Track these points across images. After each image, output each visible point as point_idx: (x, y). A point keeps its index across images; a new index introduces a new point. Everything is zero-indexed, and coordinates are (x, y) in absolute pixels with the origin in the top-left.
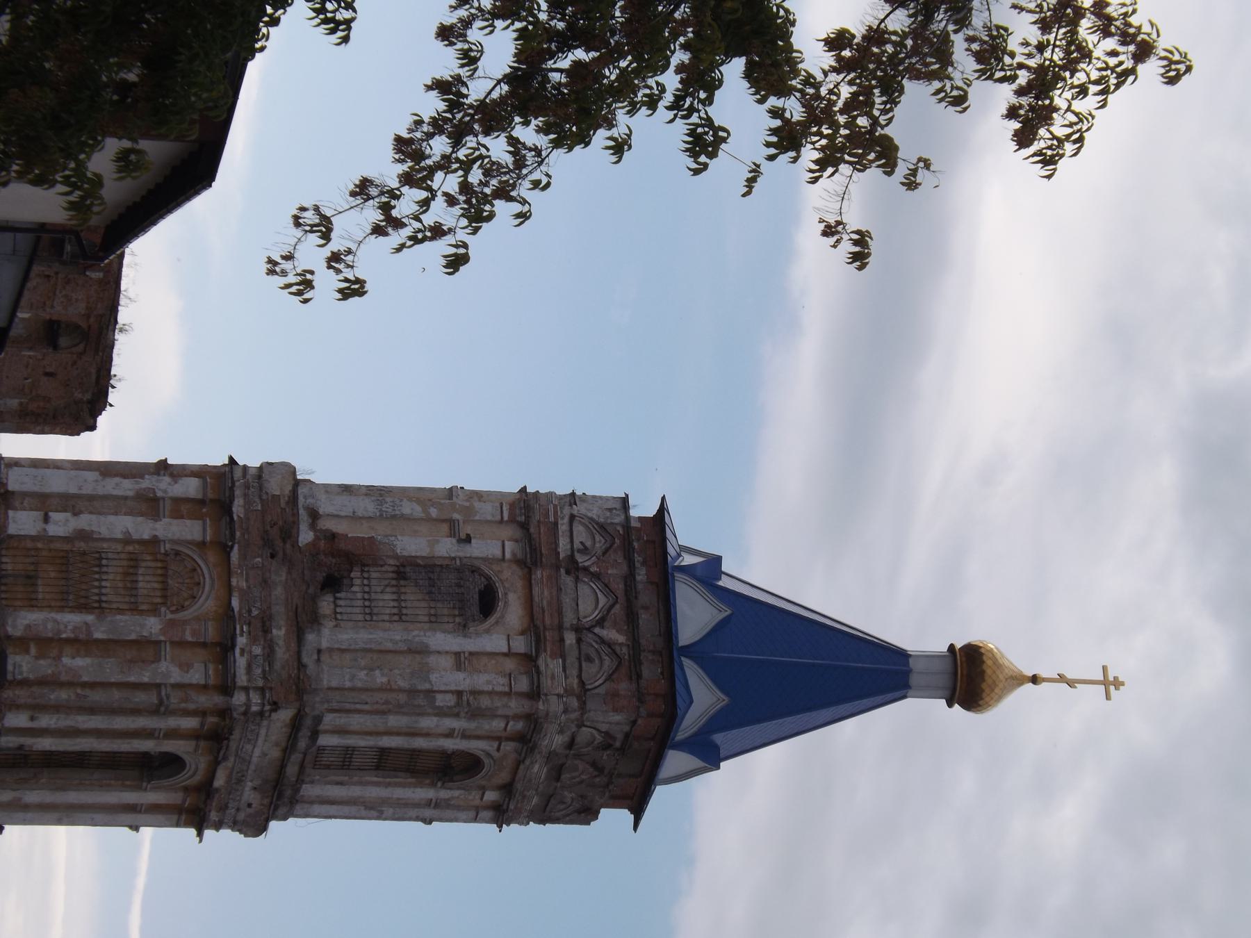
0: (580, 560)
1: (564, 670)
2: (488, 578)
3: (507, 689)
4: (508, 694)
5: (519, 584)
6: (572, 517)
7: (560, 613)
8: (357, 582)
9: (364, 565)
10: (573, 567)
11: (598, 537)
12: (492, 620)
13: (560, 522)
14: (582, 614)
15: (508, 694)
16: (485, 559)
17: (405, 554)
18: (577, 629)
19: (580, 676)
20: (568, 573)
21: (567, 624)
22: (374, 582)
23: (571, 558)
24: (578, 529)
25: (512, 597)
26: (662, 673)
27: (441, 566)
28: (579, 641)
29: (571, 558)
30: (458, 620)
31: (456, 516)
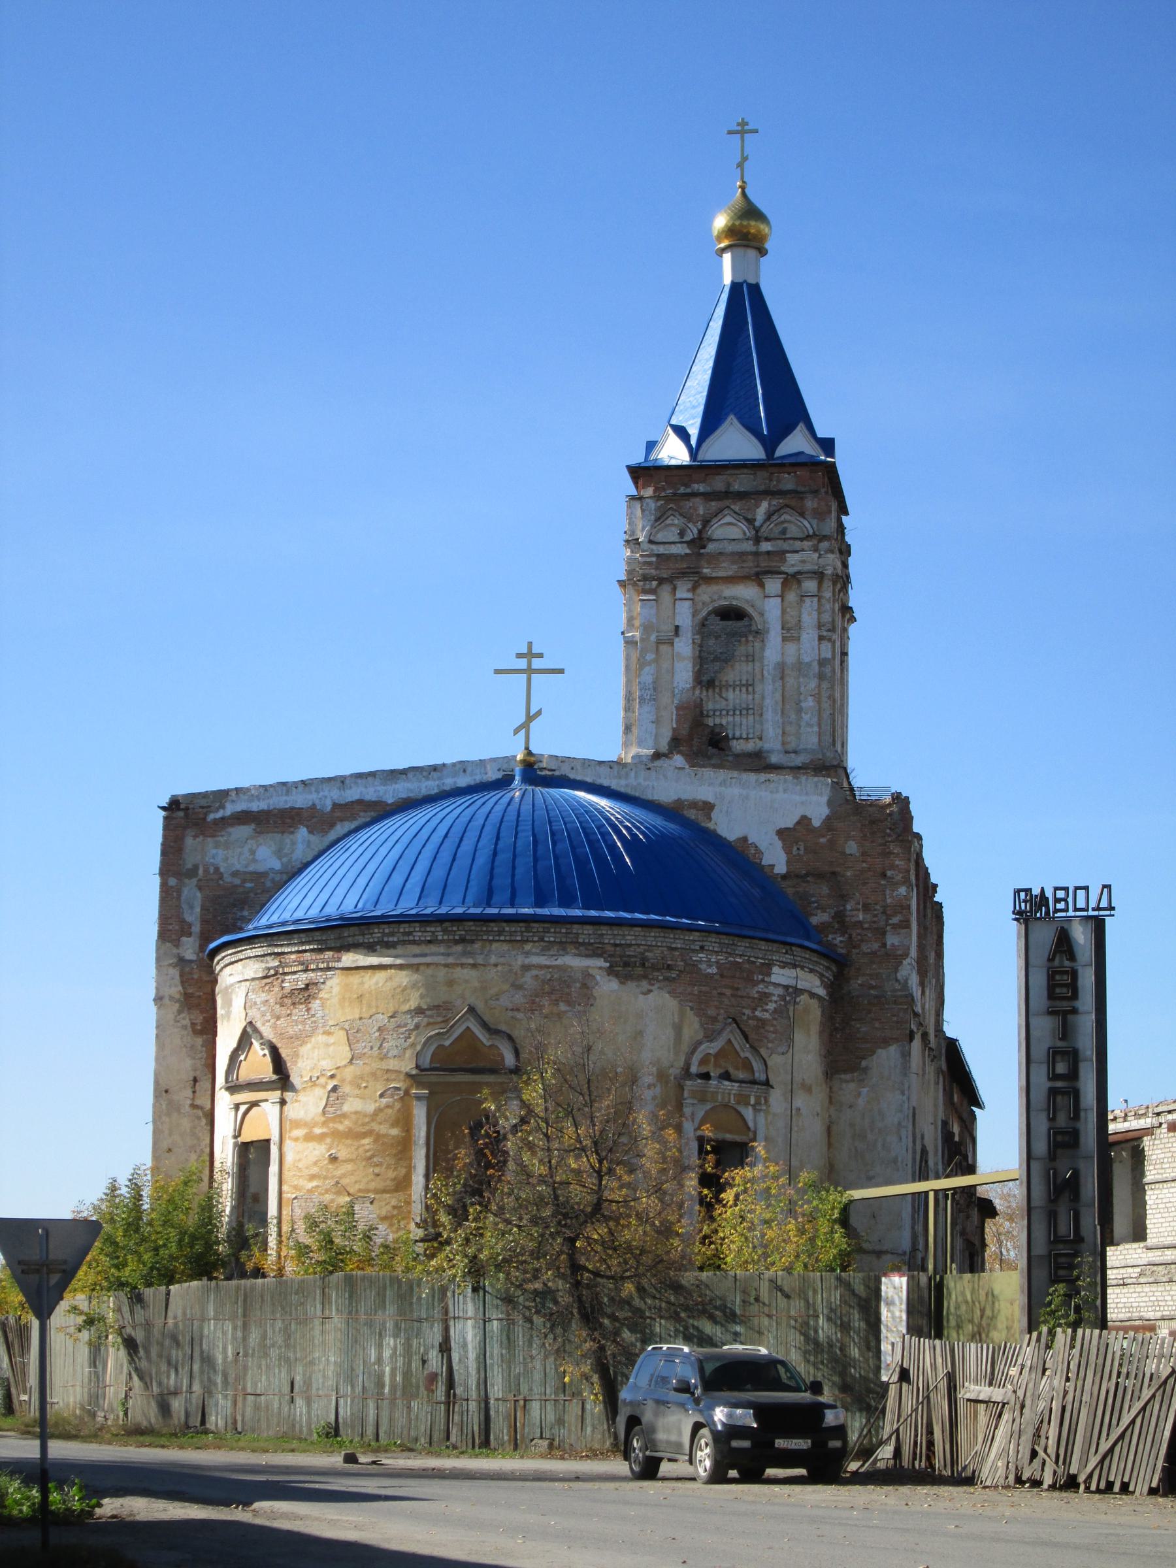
0: (691, 537)
1: (797, 552)
2: (709, 614)
3: (816, 599)
4: (820, 598)
5: (714, 588)
6: (651, 542)
8: (718, 721)
9: (702, 713)
10: (699, 542)
11: (669, 521)
12: (750, 610)
13: (656, 552)
14: (741, 536)
15: (820, 598)
17: (691, 680)
18: (757, 540)
19: (802, 540)
20: (704, 547)
21: (754, 549)
22: (718, 707)
23: (690, 543)
24: (660, 537)
26: (789, 473)
27: (700, 651)
28: (767, 539)
29: (690, 543)
30: (751, 638)
31: (653, 638)
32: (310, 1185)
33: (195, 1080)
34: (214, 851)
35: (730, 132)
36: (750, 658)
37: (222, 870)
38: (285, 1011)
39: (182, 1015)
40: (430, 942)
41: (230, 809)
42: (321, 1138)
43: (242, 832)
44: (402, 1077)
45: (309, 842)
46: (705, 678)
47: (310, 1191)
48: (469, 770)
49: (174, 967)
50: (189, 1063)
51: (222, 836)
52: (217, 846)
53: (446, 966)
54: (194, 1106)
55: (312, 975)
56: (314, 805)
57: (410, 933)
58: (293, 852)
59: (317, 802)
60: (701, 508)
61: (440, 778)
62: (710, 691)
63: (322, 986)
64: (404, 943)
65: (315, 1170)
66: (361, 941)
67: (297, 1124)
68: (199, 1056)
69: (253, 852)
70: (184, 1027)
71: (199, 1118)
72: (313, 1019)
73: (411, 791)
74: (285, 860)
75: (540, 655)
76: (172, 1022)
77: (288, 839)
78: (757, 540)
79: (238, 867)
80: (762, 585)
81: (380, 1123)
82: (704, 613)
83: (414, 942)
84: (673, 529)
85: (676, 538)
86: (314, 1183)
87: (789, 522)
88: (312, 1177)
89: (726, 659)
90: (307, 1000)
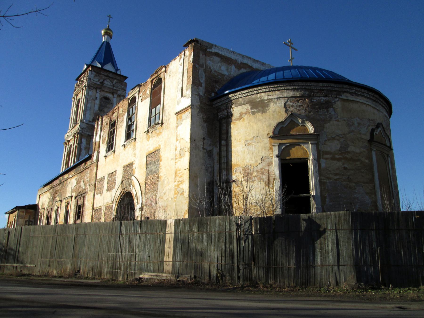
2: (102, 97)
10: (102, 83)
14: (110, 85)
16: (100, 96)
19: (121, 89)
20: (103, 84)
23: (101, 83)
24: (94, 80)
25: (106, 94)
28: (115, 87)
29: (101, 83)
31: (91, 98)
33: (204, 138)
34: (209, 62)
35: (107, 16)
37: (212, 69)
39: (199, 114)
40: (368, 98)
41: (213, 50)
42: (339, 160)
43: (217, 59)
45: (235, 70)
47: (336, 180)
49: (198, 96)
51: (211, 58)
52: (210, 60)
54: (203, 148)
56: (236, 60)
57: (363, 93)
59: (237, 60)
60: (104, 77)
62: (101, 112)
63: (334, 104)
64: (362, 95)
65: (338, 172)
66: (349, 91)
69: (220, 67)
70: (200, 118)
74: (229, 73)
78: (113, 86)
79: (216, 70)
80: (113, 95)
82: (102, 97)
83: (364, 96)
84: (97, 79)
85: (98, 81)
86: (338, 177)
87: (119, 85)
88: (336, 174)
89: (105, 107)
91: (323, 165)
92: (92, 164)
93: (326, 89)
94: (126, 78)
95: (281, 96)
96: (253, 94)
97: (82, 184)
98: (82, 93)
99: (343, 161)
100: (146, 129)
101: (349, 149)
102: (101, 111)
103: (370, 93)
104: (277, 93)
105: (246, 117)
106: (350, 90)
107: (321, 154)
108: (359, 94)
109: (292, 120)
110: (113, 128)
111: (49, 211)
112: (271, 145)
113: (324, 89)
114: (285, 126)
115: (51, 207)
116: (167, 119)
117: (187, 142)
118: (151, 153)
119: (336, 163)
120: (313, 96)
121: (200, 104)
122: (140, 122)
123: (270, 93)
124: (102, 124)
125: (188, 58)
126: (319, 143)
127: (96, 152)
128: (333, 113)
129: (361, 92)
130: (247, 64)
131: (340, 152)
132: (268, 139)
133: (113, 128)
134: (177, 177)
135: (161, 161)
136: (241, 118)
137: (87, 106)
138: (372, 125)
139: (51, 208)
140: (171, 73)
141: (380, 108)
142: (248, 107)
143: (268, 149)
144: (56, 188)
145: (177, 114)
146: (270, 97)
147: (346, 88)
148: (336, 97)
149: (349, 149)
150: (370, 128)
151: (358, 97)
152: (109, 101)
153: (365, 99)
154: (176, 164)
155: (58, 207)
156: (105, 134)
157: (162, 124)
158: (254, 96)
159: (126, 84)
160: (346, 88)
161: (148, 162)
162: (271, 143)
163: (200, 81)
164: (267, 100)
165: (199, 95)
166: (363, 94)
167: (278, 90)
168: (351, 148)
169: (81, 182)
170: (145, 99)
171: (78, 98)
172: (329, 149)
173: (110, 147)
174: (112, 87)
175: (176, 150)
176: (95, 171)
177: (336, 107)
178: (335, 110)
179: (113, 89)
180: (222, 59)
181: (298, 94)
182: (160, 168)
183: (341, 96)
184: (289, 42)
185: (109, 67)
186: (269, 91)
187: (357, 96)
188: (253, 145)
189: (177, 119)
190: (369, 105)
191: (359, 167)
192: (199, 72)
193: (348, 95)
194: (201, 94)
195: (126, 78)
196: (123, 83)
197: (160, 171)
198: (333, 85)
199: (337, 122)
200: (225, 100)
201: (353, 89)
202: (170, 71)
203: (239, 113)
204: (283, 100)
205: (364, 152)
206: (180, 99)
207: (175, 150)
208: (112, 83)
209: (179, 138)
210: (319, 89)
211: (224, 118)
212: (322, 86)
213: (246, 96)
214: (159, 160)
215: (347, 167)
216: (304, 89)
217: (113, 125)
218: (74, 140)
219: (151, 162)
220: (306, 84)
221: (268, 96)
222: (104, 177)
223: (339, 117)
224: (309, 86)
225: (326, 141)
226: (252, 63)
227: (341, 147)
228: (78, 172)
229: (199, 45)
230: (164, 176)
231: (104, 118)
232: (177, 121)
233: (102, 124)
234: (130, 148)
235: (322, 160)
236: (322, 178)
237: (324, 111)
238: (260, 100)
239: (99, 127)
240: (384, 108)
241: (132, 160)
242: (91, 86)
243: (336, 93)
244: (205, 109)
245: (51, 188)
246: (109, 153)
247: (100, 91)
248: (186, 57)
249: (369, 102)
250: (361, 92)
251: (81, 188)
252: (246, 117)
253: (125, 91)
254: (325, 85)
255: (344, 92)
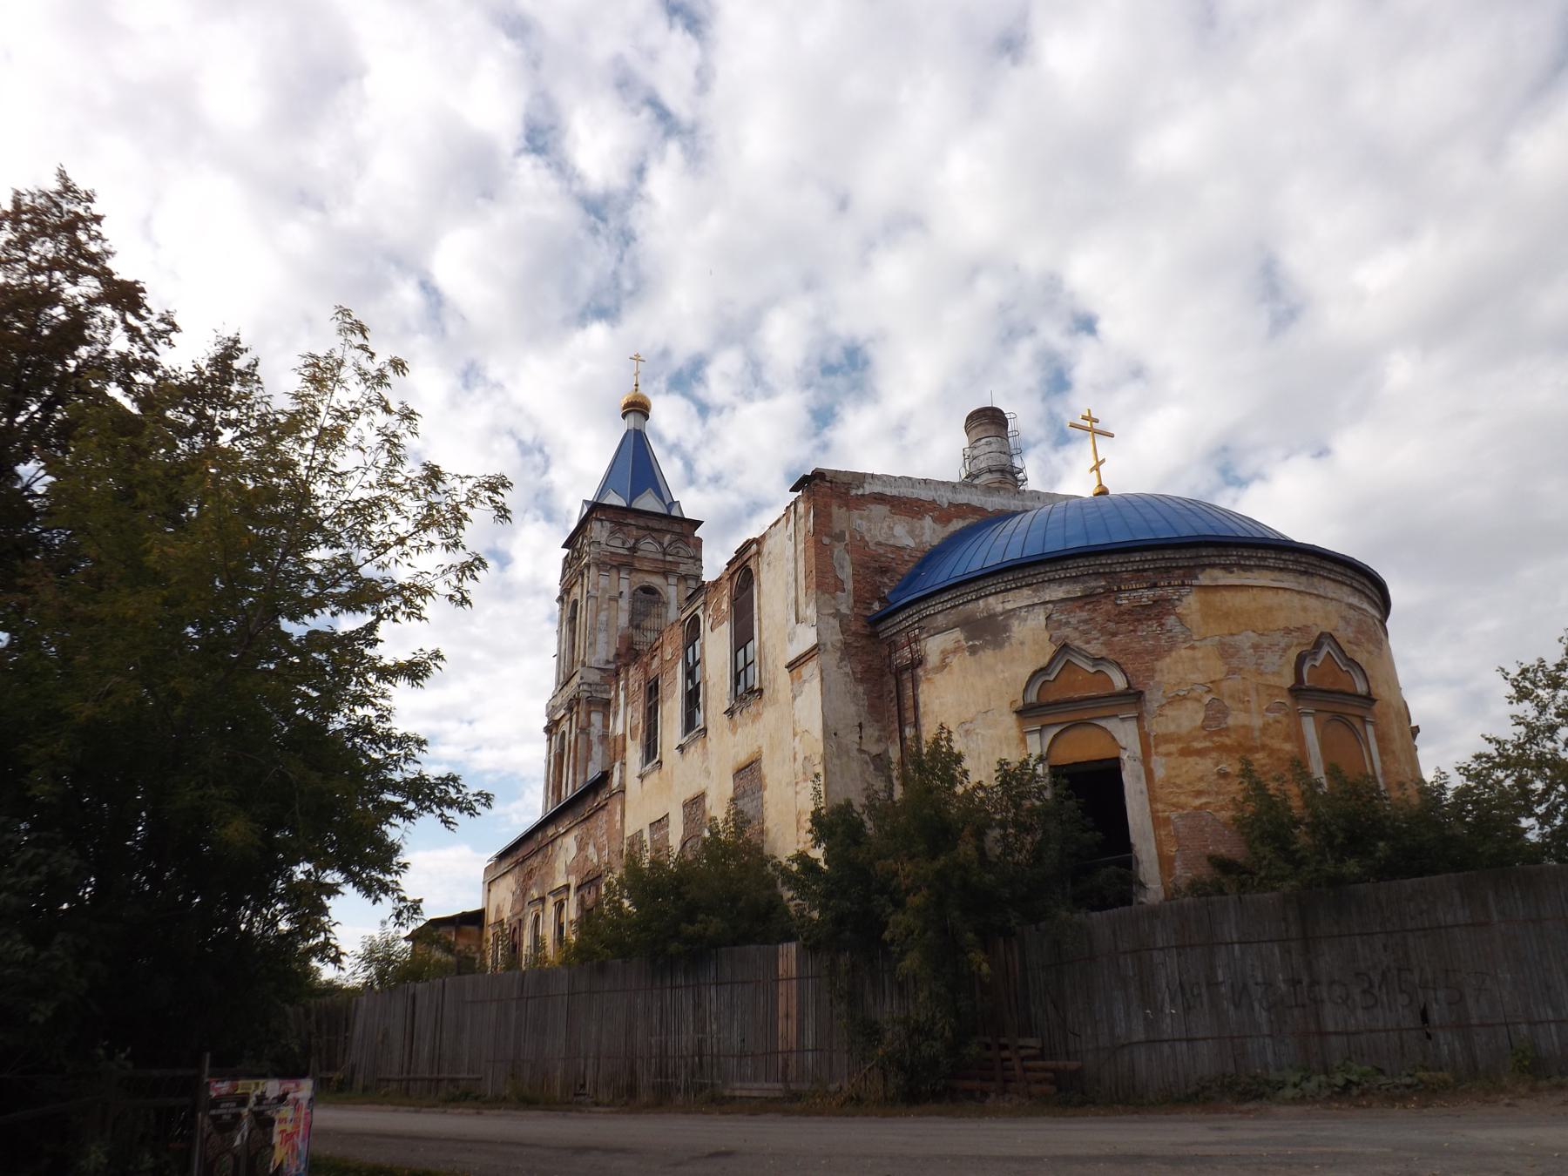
5: (640, 575)
7: (657, 560)
10: (633, 549)
16: (630, 587)
18: (665, 554)
23: (628, 549)
24: (611, 543)
29: (628, 549)
31: (607, 596)
32: (1197, 802)
34: (859, 522)
36: (659, 616)
37: (867, 538)
38: (1123, 627)
39: (844, 663)
40: (1281, 570)
42: (1201, 753)
43: (880, 510)
44: (1285, 693)
46: (635, 623)
47: (1200, 808)
48: (1042, 498)
49: (834, 618)
50: (853, 709)
53: (1299, 592)
54: (861, 751)
55: (1159, 592)
57: (1265, 559)
58: (923, 534)
59: (937, 499)
61: (1023, 500)
63: (1177, 603)
64: (1258, 567)
65: (1202, 786)
67: (1167, 739)
68: (861, 703)
69: (891, 529)
71: (867, 763)
72: (1169, 634)
73: (1003, 505)
74: (917, 540)
75: (1097, 421)
76: (835, 669)
77: (917, 524)
78: (665, 554)
79: (880, 539)
80: (666, 578)
81: (1272, 738)
83: (1267, 568)
86: (1203, 800)
88: (1199, 794)
89: (647, 615)
90: (1159, 618)
91: (1160, 773)
92: (610, 797)
93: (1152, 566)
94: (697, 524)
95: (1036, 601)
96: (969, 601)
97: (591, 850)
98: (582, 585)
99: (1215, 755)
100: (727, 707)
101: (1231, 721)
102: (637, 627)
103: (1283, 557)
104: (1026, 592)
105: (955, 661)
106: (1223, 558)
107: (1152, 744)
108: (1250, 566)
109: (1068, 660)
110: (654, 700)
111: (515, 929)
112: (1021, 731)
113: (1146, 566)
114: (1052, 678)
115: (520, 916)
116: (772, 677)
117: (817, 740)
118: (742, 769)
119: (1197, 764)
120: (1120, 590)
121: (841, 637)
122: (714, 685)
123: (1010, 595)
124: (626, 687)
125: (803, 520)
126: (1145, 715)
127: (617, 765)
128: (1178, 629)
129: (1256, 557)
130: (968, 505)
131: (1205, 733)
132: (1014, 716)
133: (654, 700)
134: (801, 831)
135: (765, 789)
136: (943, 666)
137: (596, 616)
138: (1299, 644)
139: (520, 920)
140: (771, 557)
141: (1329, 589)
142: (957, 634)
143: (1016, 742)
144: (528, 863)
145: (792, 666)
146: (1009, 606)
147: (1208, 556)
148: (1183, 585)
149: (1231, 721)
150: (1293, 654)
151: (1249, 574)
152: (657, 596)
153: (1277, 575)
154: (798, 796)
155: (537, 917)
156: (636, 715)
157: (761, 691)
158: (970, 606)
159: (700, 540)
160: (1208, 556)
161: (740, 791)
162: (1021, 726)
163: (836, 577)
164: (1001, 614)
165: (837, 614)
166: (1262, 563)
167: (1028, 585)
168: (1236, 719)
169: (588, 844)
170: (721, 623)
171: (572, 598)
172: (1172, 728)
173: (650, 750)
174: (660, 557)
175: (795, 759)
176: (618, 817)
177: (1185, 612)
178: (1180, 618)
179: (664, 561)
180: (892, 506)
181: (1077, 590)
182: (765, 806)
183: (1197, 578)
184: (1084, 418)
185: (647, 502)
186: (1007, 590)
187: (1244, 571)
188: (977, 734)
189: (792, 680)
190: (1285, 589)
191: (1263, 766)
192: (832, 553)
193: (1218, 573)
194: (844, 610)
195: (697, 524)
196: (691, 541)
197: (766, 814)
198: (1168, 554)
199: (1190, 652)
200: (903, 620)
201: (1232, 555)
202: (770, 553)
203: (938, 652)
204: (1042, 610)
205: (1278, 722)
206: (794, 627)
207: (792, 759)
208: (661, 544)
209: (798, 730)
210: (1133, 570)
211: (906, 668)
212: (1141, 561)
213: (952, 607)
214: (761, 787)
215: (1229, 770)
216: (1093, 574)
217: (653, 691)
218: (571, 719)
219: (745, 791)
220: (1098, 562)
221: (1003, 602)
222: (641, 831)
223: (1195, 637)
224: (1107, 564)
225: (1162, 706)
226: (982, 498)
227: (1206, 718)
228: (579, 819)
229: (828, 484)
230: (775, 829)
231: (631, 673)
232: (792, 684)
233: (626, 687)
234: (694, 752)
235: (1154, 758)
236: (1160, 806)
237: (1151, 626)
238: (985, 614)
239: (622, 694)
240: (1343, 583)
241: (703, 787)
242: (604, 563)
243: (1181, 572)
244: (857, 647)
245: (517, 864)
246: (649, 766)
247: (629, 574)
248: (801, 518)
249: (1289, 581)
250: (1256, 557)
251: (589, 863)
252: (955, 661)
253: (698, 563)
254: (1149, 558)
255: (1204, 567)
